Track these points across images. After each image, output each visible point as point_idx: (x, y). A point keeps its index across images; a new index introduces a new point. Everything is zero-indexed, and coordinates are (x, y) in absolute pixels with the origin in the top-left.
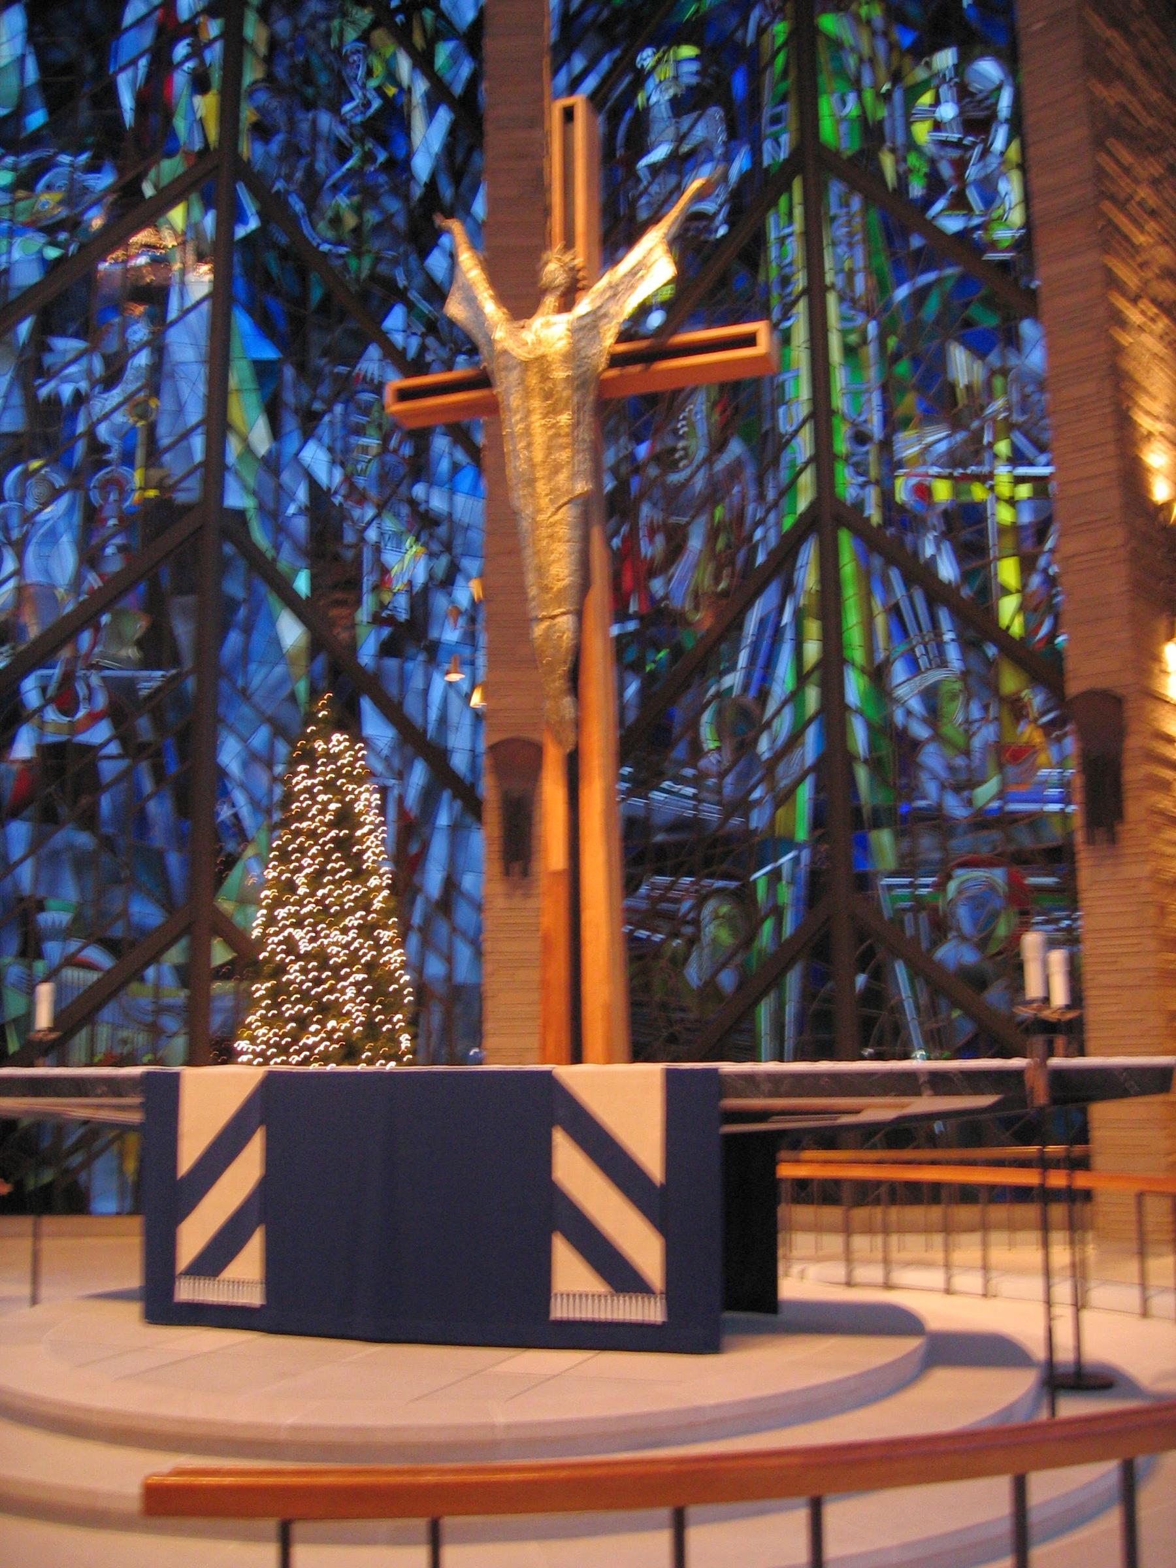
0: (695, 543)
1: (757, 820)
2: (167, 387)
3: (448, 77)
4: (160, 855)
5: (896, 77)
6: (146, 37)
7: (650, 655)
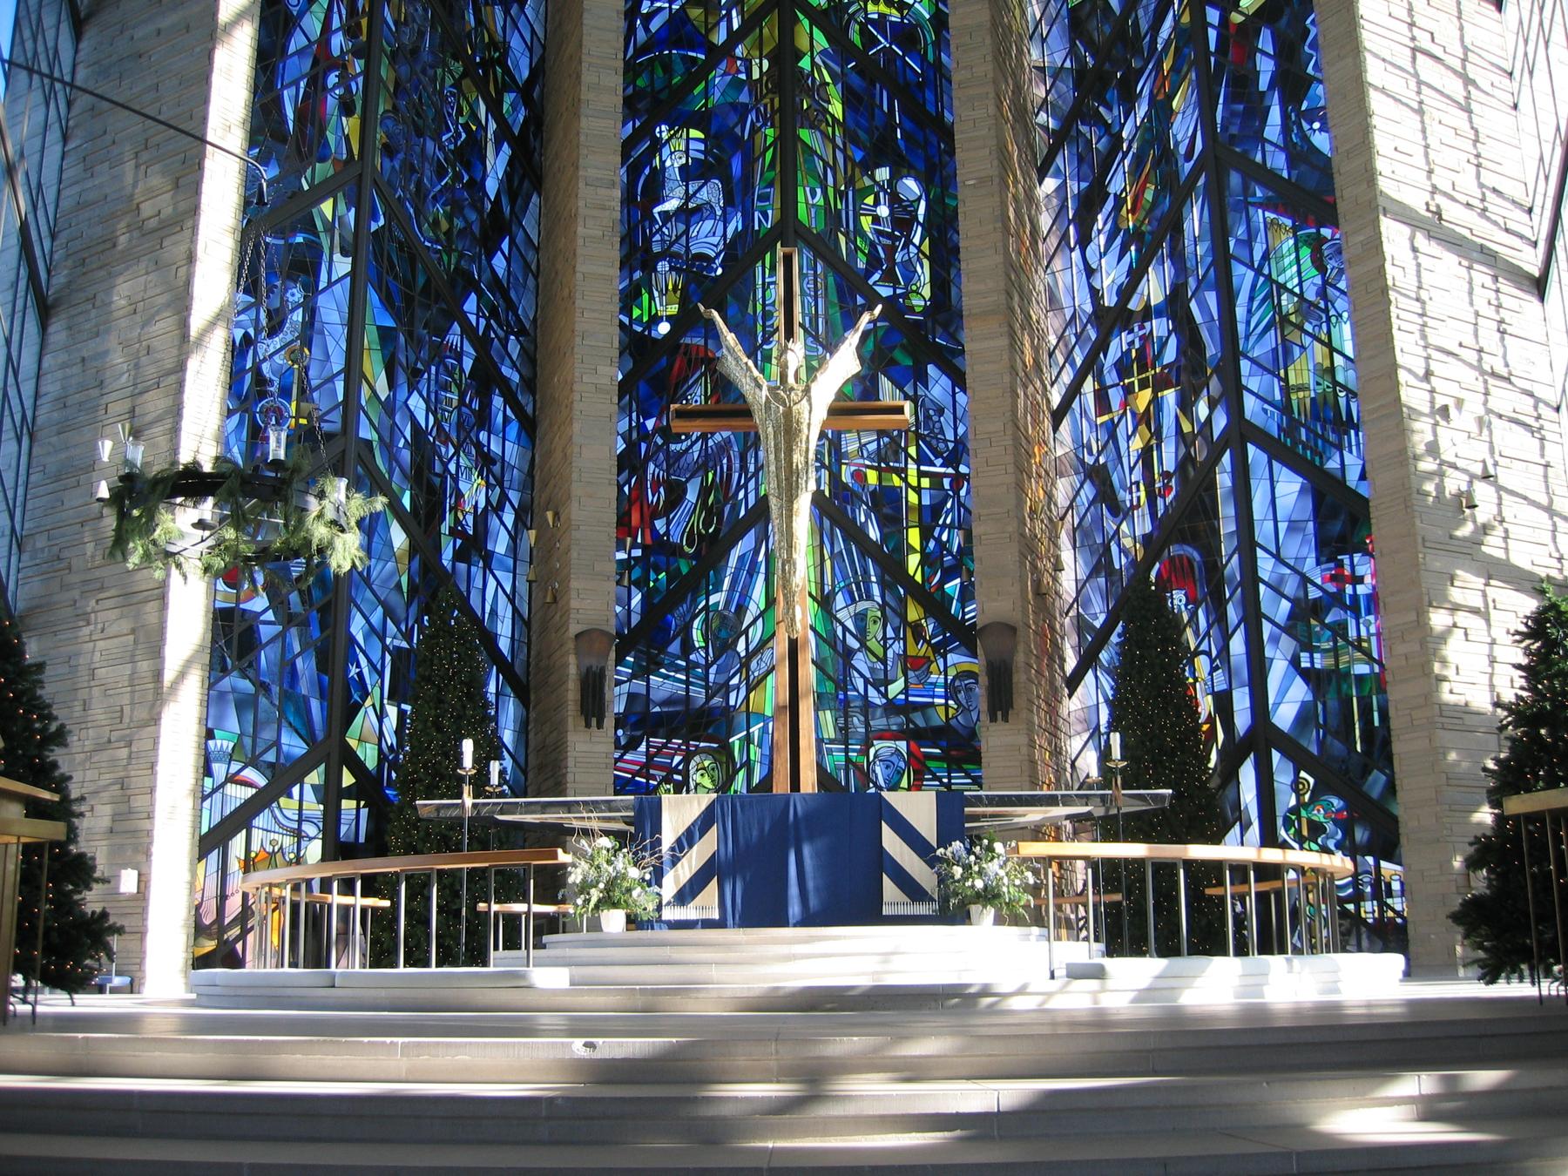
0: (692, 496)
2: (316, 339)
3: (510, 121)
4: (306, 700)
5: (850, 182)
6: (307, 65)
7: (653, 576)
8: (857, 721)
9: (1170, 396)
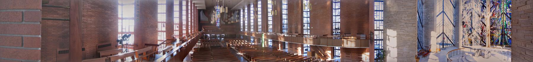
0: (497, 13)
8: (507, 30)
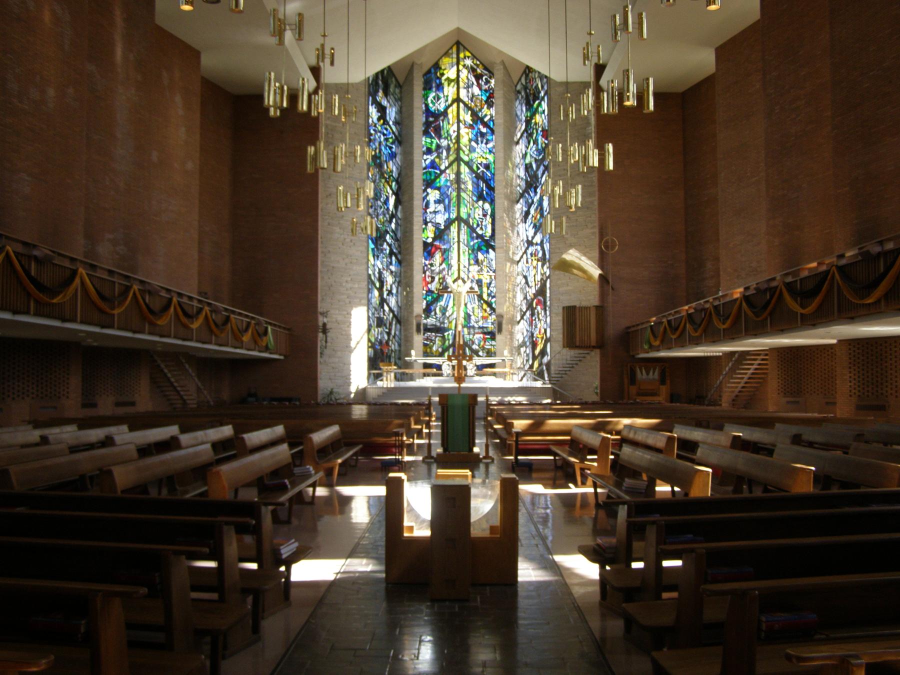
1: (446, 326)
5: (473, 206)
9: (540, 264)
